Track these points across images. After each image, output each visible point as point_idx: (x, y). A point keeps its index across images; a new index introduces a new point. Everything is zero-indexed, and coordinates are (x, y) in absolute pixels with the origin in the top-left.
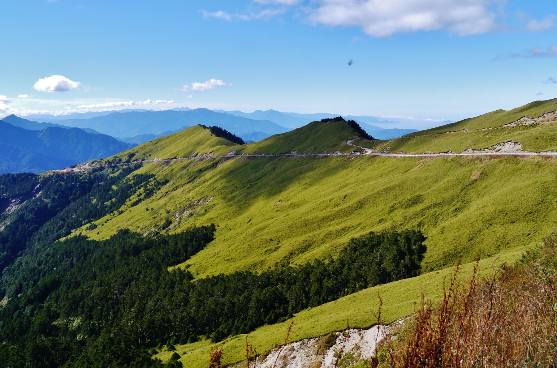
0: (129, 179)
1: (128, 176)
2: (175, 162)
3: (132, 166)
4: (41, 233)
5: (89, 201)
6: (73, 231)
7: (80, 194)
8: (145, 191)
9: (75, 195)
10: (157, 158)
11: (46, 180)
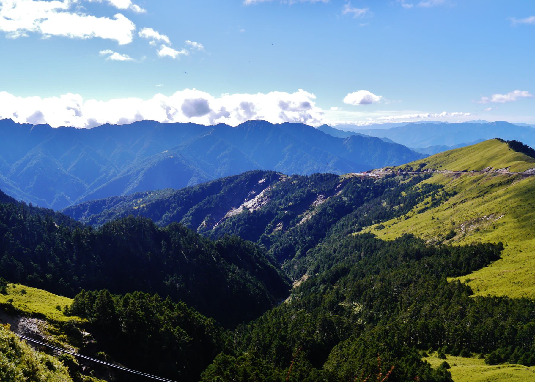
1: (418, 185)
2: (466, 175)
3: (422, 175)
4: (338, 226)
5: (380, 204)
6: (364, 228)
7: (372, 197)
8: (433, 200)
9: (369, 196)
11: (347, 181)
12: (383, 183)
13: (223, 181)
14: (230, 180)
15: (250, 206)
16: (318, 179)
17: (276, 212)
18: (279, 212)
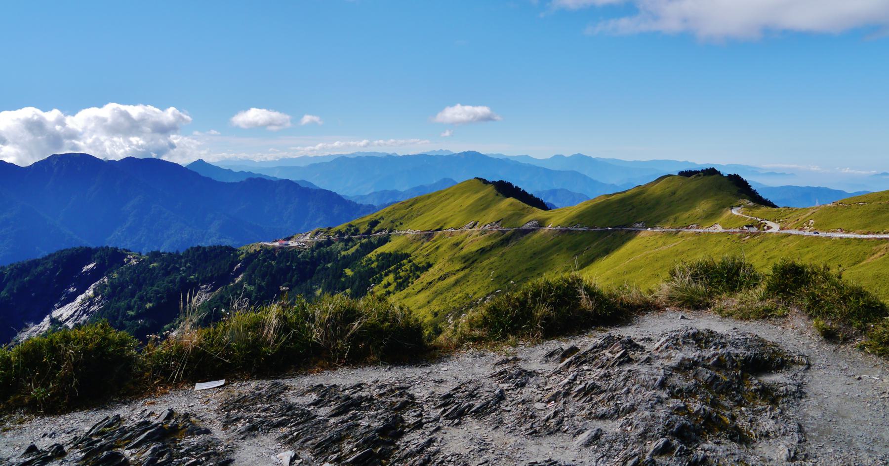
0: (370, 259)
1: (369, 255)
2: (441, 236)
3: (375, 237)
7: (297, 282)
8: (396, 279)
10: (412, 230)
11: (251, 257)
12: (313, 257)
13: (7, 272)
14: (22, 270)
15: (65, 317)
16: (199, 256)
17: (121, 323)
18: (127, 323)
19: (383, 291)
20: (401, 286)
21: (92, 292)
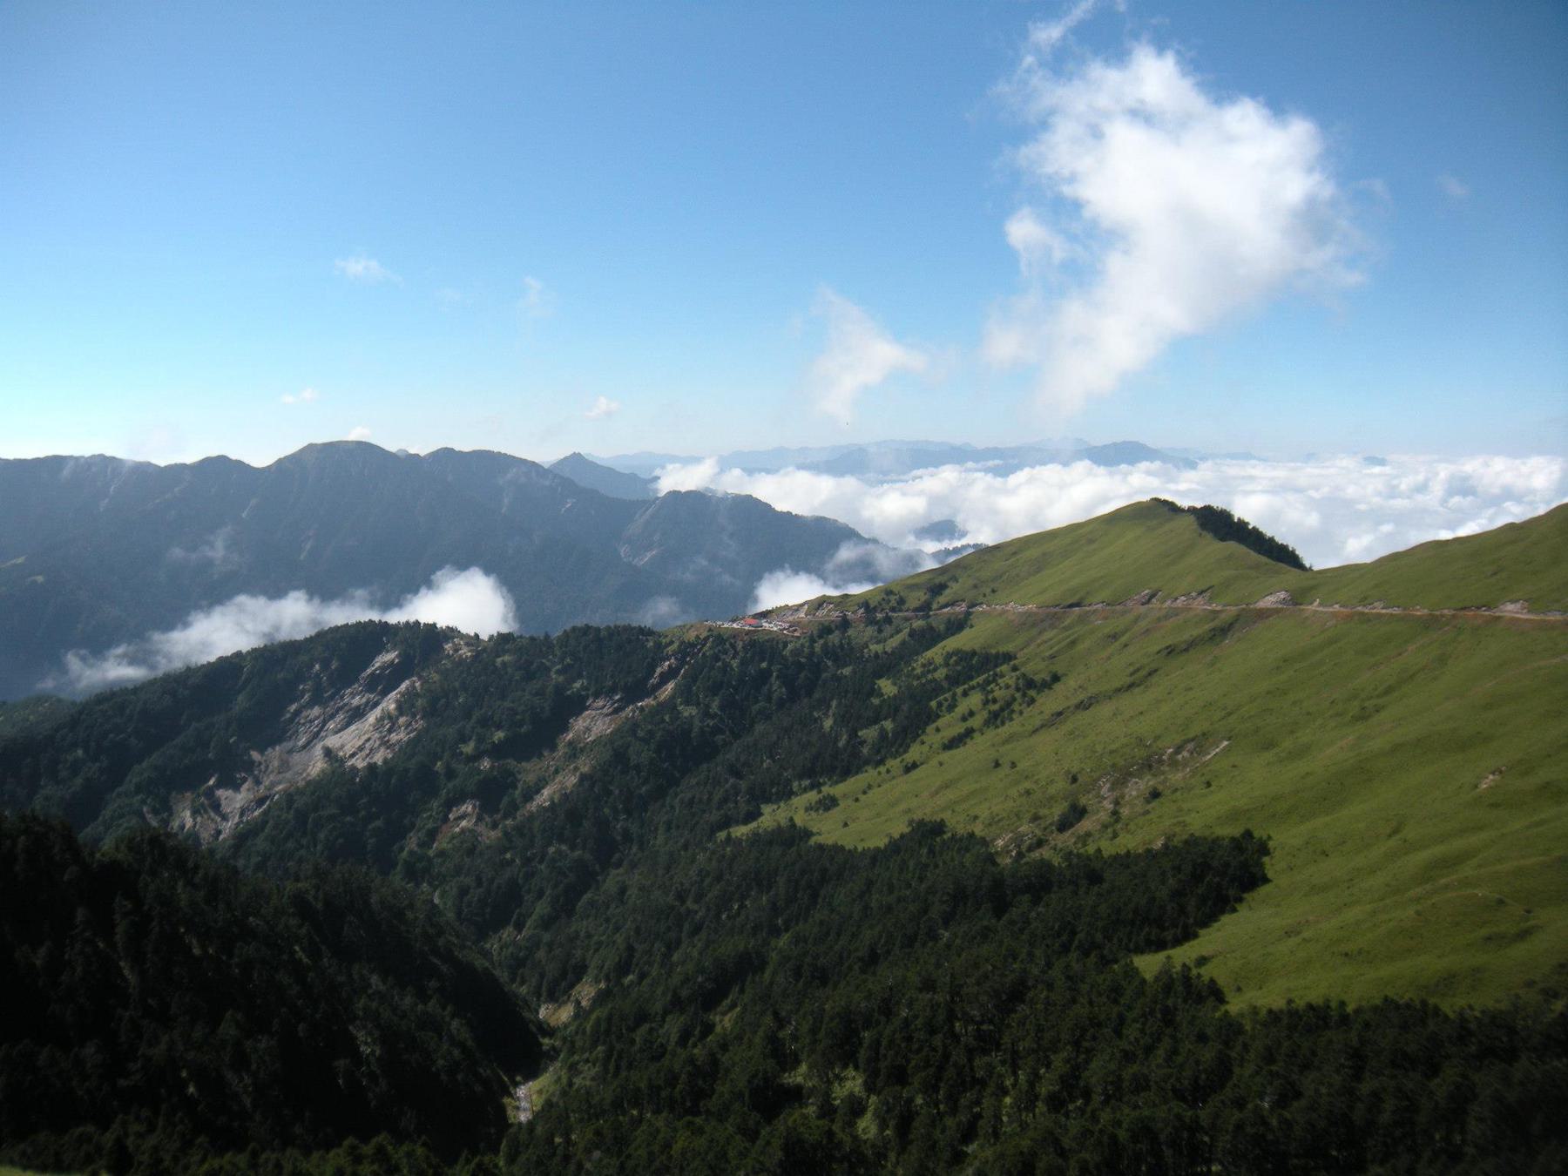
1: (929, 654)
2: (1082, 619)
3: (942, 614)
4: (672, 807)
6: (767, 809)
8: (986, 703)
15: (349, 750)
19: (960, 729)
20: (995, 719)
21: (393, 706)
